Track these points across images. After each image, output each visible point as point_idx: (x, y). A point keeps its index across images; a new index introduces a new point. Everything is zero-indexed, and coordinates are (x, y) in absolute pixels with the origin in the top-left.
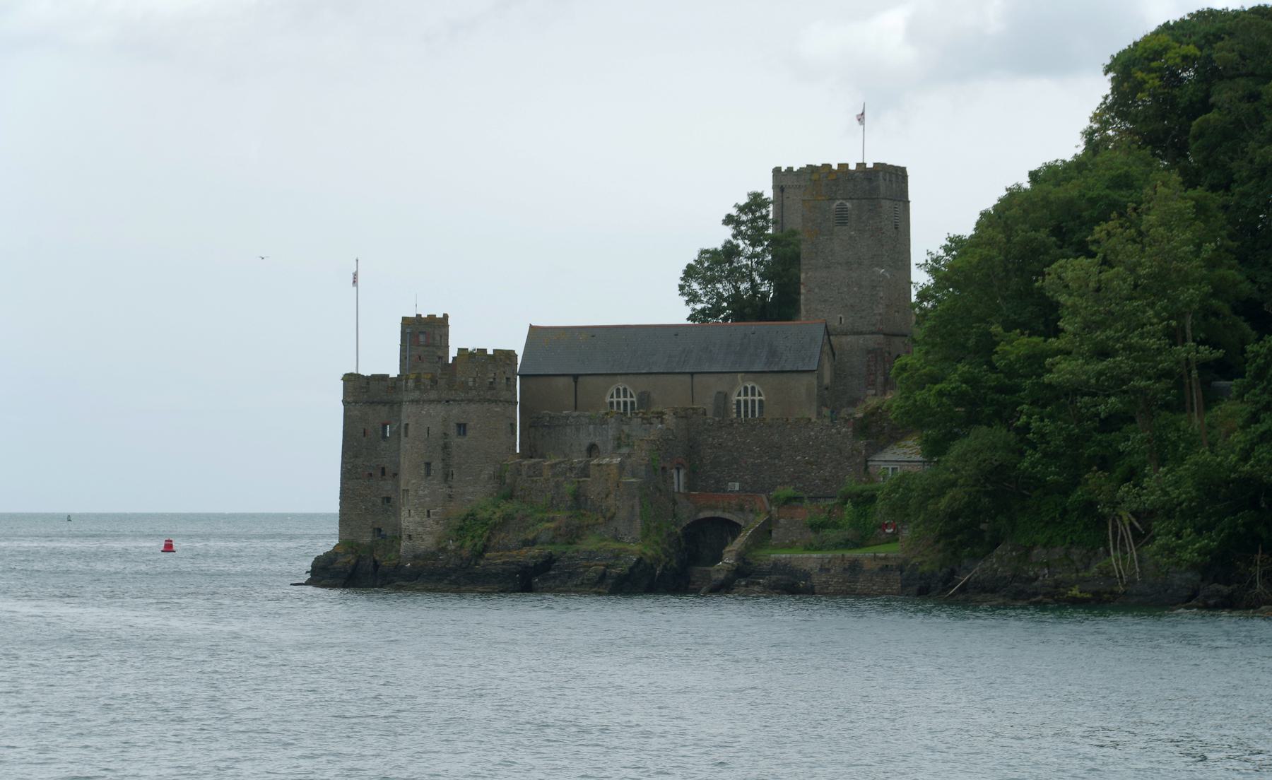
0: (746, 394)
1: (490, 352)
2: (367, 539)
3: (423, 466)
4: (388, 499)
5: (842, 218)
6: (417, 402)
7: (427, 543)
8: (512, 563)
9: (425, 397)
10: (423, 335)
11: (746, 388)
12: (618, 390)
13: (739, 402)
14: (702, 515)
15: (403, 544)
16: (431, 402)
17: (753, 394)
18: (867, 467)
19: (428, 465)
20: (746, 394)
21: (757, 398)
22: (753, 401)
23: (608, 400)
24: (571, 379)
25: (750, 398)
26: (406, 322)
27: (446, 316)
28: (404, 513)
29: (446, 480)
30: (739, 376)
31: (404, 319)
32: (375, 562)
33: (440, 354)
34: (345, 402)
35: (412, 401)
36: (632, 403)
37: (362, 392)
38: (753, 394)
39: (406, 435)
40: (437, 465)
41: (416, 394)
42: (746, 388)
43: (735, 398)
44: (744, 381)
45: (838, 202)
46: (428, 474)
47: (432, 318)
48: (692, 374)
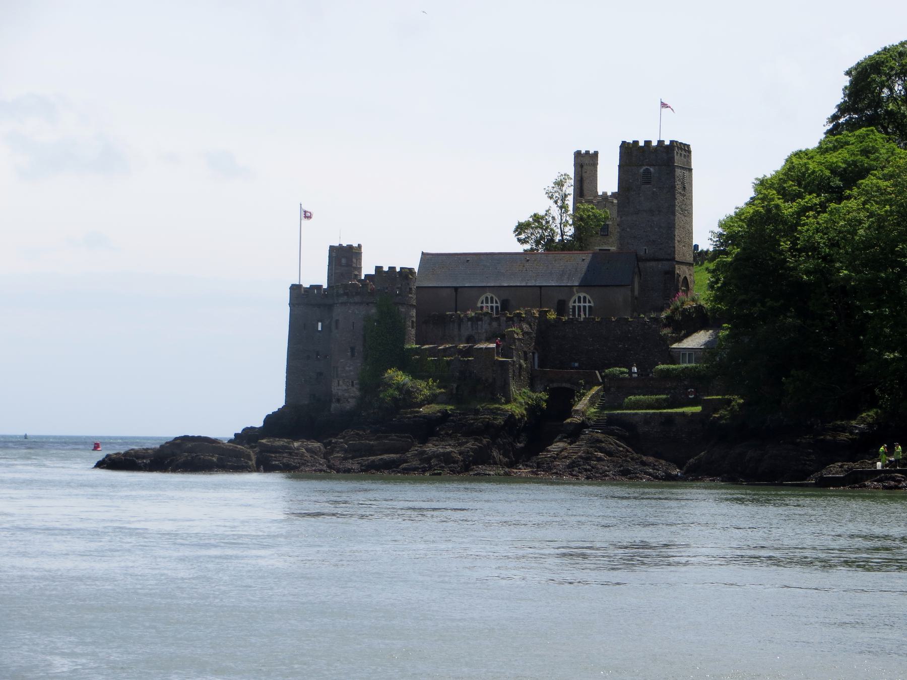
0: (579, 302)
1: (398, 270)
4: (321, 374)
7: (350, 405)
8: (420, 417)
10: (344, 258)
12: (487, 298)
13: (574, 307)
16: (356, 303)
17: (585, 302)
20: (579, 302)
21: (587, 304)
22: (585, 307)
23: (479, 305)
25: (582, 304)
26: (332, 248)
27: (360, 246)
28: (335, 383)
31: (331, 247)
33: (356, 273)
35: (342, 303)
36: (497, 307)
37: (302, 299)
38: (585, 302)
39: (337, 328)
41: (345, 299)
42: (579, 298)
43: (571, 304)
46: (353, 355)
47: (350, 247)
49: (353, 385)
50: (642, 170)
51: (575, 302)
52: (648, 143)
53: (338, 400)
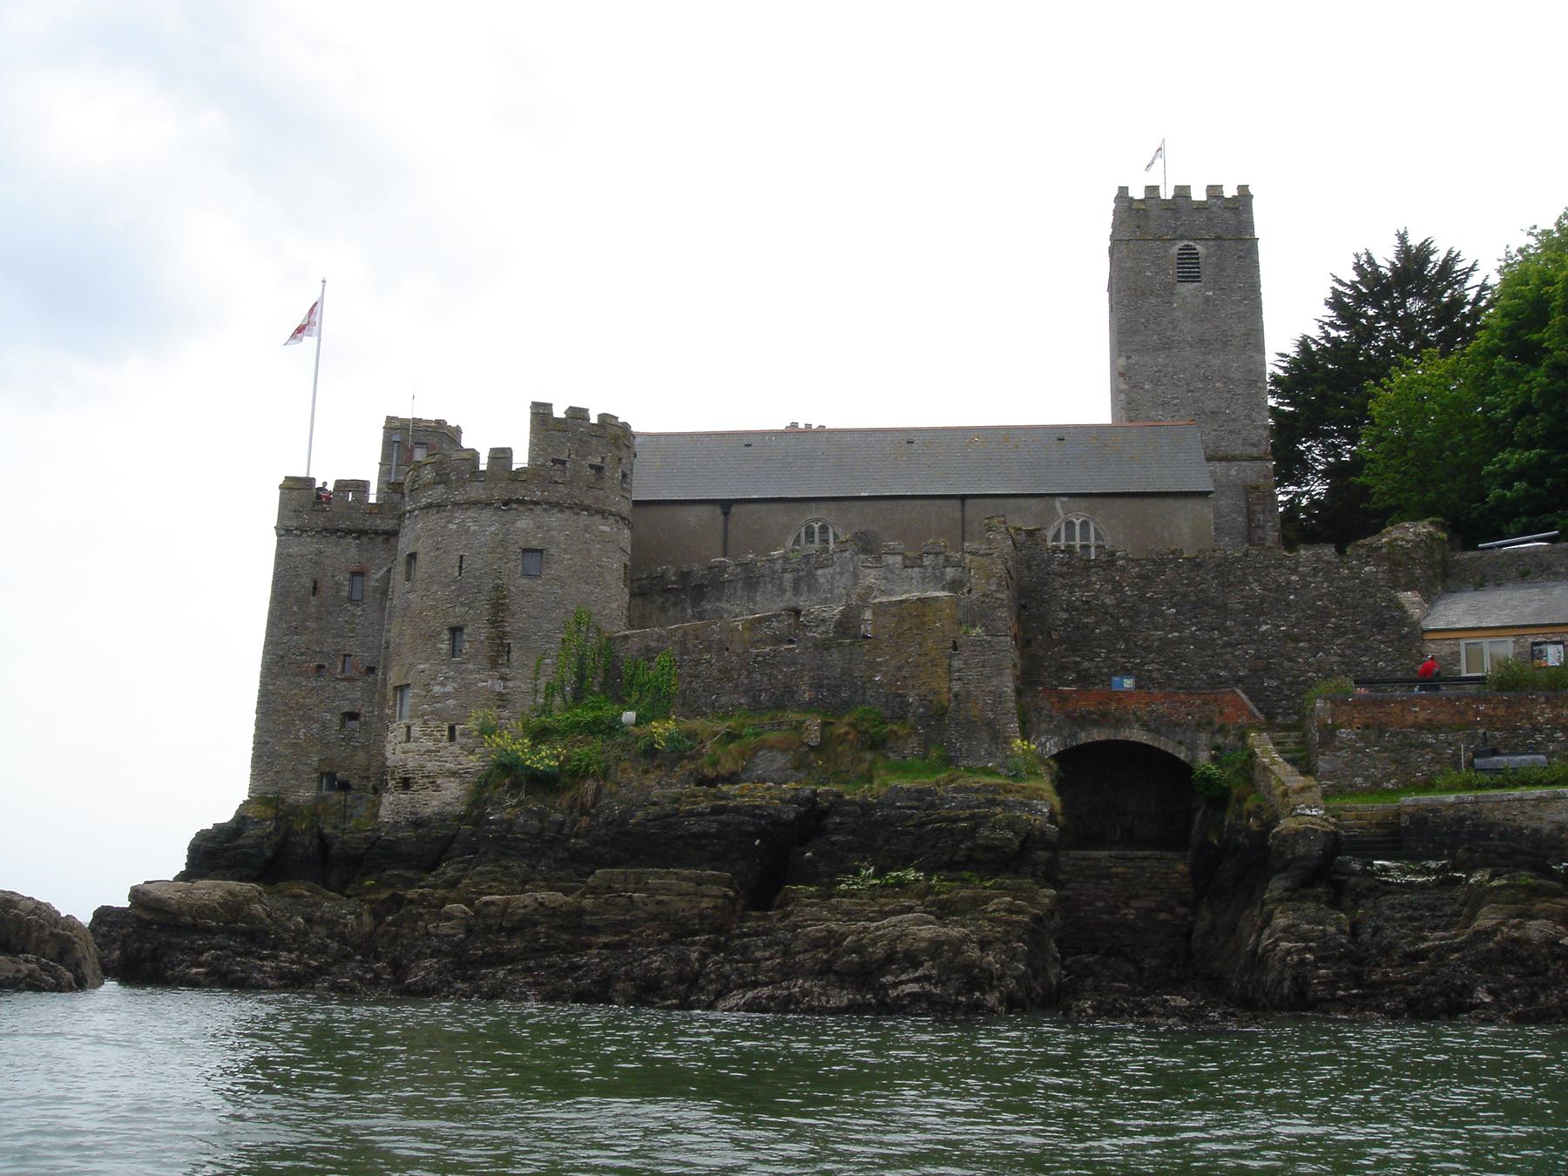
0: (1070, 536)
1: (594, 420)
2: (305, 794)
3: (446, 636)
4: (353, 716)
5: (1189, 267)
6: (439, 506)
7: (449, 796)
9: (459, 497)
11: (1070, 525)
14: (1084, 737)
15: (387, 799)
19: (455, 631)
20: (1070, 536)
24: (718, 510)
28: (395, 735)
29: (494, 664)
30: (1057, 503)
31: (389, 419)
32: (322, 837)
34: (284, 531)
35: (429, 506)
40: (478, 632)
41: (437, 494)
42: (1070, 525)
44: (1067, 511)
45: (1181, 244)
46: (454, 651)
48: (963, 498)
49: (452, 738)
50: (1175, 249)
52: (1182, 192)
53: (406, 784)
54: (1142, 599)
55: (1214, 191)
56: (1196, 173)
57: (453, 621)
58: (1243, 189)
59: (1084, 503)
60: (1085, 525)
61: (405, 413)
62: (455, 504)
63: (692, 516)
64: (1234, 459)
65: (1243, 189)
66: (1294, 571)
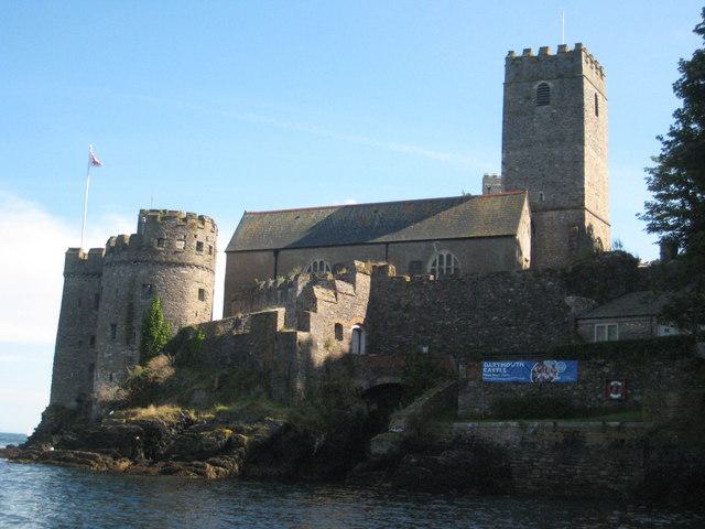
0: (441, 263)
5: (544, 96)
11: (441, 256)
14: (379, 382)
16: (121, 262)
18: (576, 326)
19: (114, 326)
20: (441, 263)
34: (67, 274)
40: (121, 328)
42: (441, 256)
50: (536, 87)
51: (434, 264)
52: (543, 50)
54: (434, 303)
55: (562, 48)
56: (549, 37)
57: (112, 321)
58: (578, 45)
59: (448, 243)
60: (449, 256)
61: (147, 208)
62: (116, 263)
63: (261, 257)
64: (562, 209)
65: (578, 45)
66: (511, 285)
